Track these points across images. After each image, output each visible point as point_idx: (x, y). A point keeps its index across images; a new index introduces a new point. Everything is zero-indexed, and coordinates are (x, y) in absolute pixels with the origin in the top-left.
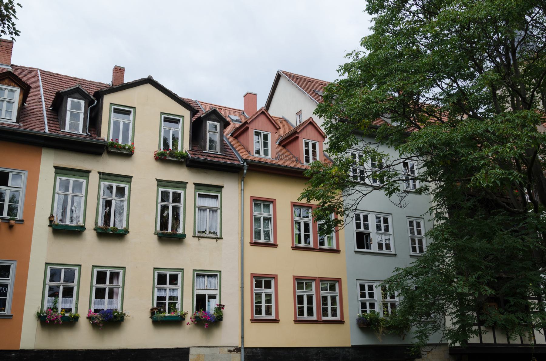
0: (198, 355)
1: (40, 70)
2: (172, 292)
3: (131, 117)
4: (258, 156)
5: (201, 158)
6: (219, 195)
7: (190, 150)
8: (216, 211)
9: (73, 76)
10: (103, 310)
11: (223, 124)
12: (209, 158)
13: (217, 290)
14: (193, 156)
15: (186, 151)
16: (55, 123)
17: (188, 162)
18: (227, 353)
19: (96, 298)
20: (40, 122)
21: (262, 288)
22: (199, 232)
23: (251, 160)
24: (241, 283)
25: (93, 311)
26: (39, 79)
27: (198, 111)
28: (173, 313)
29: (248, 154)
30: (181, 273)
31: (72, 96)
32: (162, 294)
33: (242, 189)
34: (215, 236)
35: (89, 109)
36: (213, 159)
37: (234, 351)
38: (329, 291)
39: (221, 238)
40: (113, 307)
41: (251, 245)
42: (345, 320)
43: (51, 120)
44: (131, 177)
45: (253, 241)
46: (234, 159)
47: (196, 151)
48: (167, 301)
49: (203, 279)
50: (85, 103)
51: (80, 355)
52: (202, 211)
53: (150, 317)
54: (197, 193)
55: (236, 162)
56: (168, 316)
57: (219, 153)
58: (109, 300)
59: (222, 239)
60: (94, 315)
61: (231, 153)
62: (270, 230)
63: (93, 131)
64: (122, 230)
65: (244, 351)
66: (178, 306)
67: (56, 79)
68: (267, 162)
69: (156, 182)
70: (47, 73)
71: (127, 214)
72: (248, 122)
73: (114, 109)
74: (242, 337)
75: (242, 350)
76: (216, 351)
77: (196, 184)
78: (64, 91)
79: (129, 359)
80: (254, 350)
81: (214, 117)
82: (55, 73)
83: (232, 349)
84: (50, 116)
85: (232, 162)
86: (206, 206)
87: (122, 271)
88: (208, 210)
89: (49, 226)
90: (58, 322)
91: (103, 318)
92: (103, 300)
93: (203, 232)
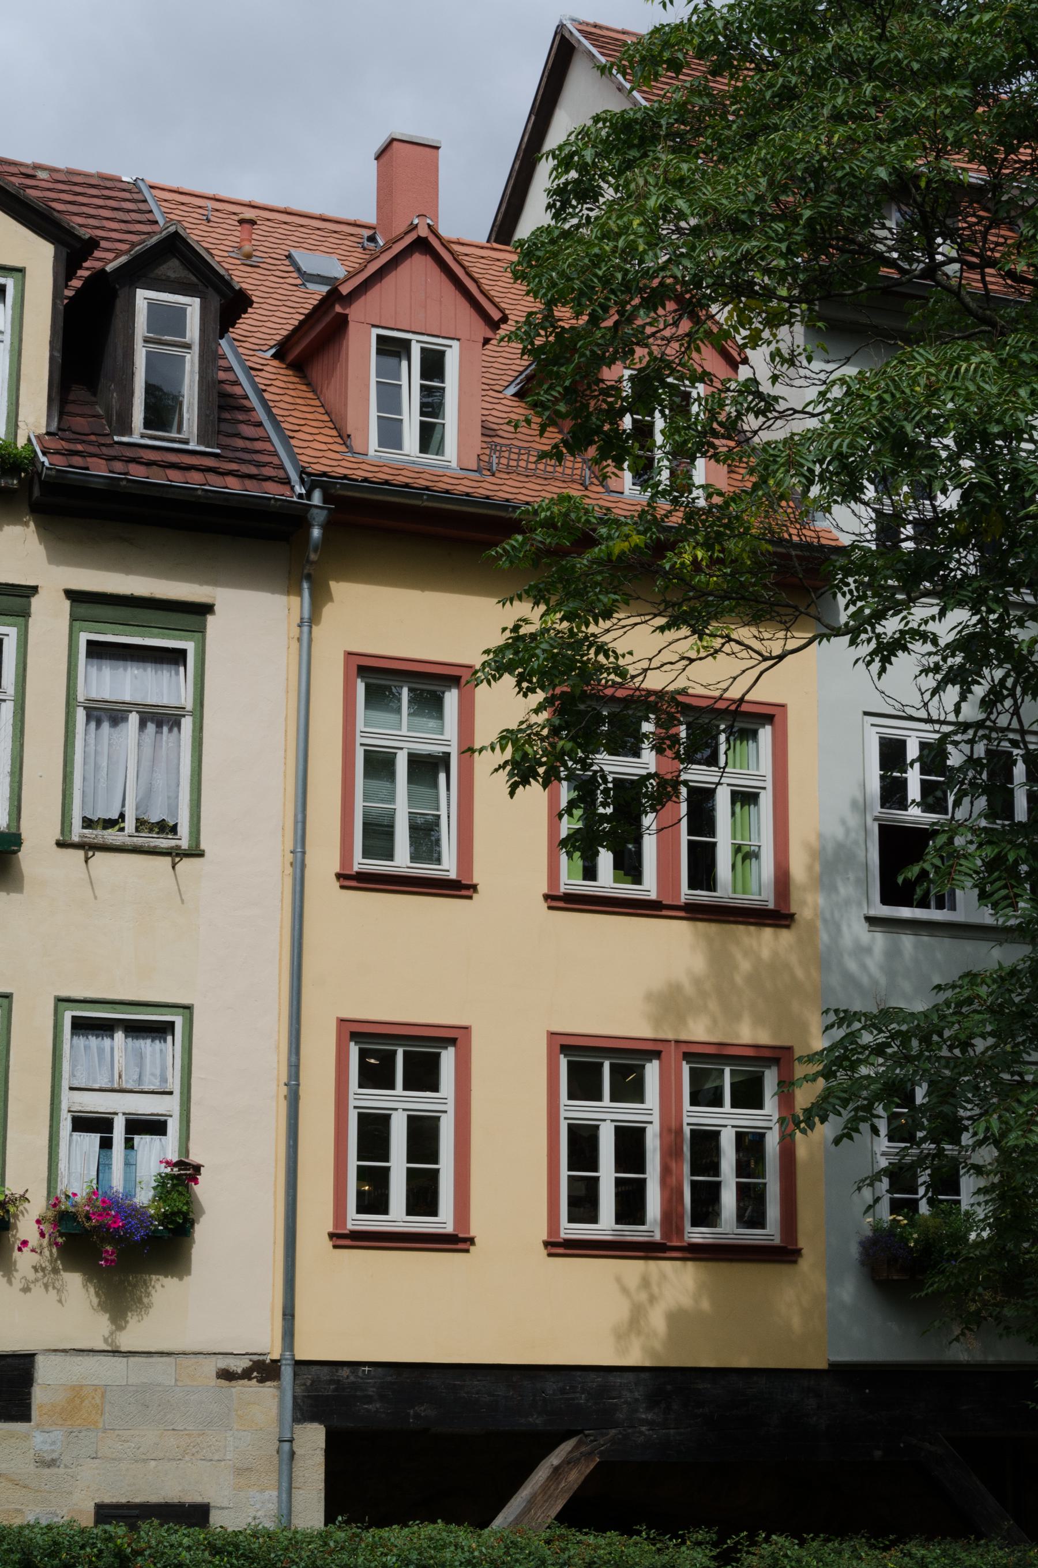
0: (73, 1388)
4: (390, 455)
5: (99, 469)
6: (189, 646)
7: (48, 433)
11: (216, 302)
12: (138, 473)
13: (171, 1093)
14: (60, 462)
15: (29, 440)
17: (36, 492)
18: (214, 1381)
21: (392, 1087)
23: (345, 477)
24: (290, 1066)
27: (93, 244)
29: (343, 448)
33: (302, 619)
34: (164, 843)
37: (246, 1374)
38: (727, 1107)
39: (196, 853)
41: (342, 887)
42: (802, 1243)
45: (356, 868)
46: (268, 471)
47: (79, 436)
49: (107, 1041)
52: (106, 726)
54: (84, 637)
55: (273, 490)
57: (192, 446)
59: (201, 854)
61: (259, 445)
62: (443, 813)
65: (296, 1375)
68: (427, 488)
72: (345, 290)
74: (289, 1314)
75: (287, 1372)
76: (160, 1371)
77: (74, 596)
80: (345, 1372)
81: (172, 268)
83: (239, 1365)
85: (254, 489)
86: (127, 698)
93: (109, 824)
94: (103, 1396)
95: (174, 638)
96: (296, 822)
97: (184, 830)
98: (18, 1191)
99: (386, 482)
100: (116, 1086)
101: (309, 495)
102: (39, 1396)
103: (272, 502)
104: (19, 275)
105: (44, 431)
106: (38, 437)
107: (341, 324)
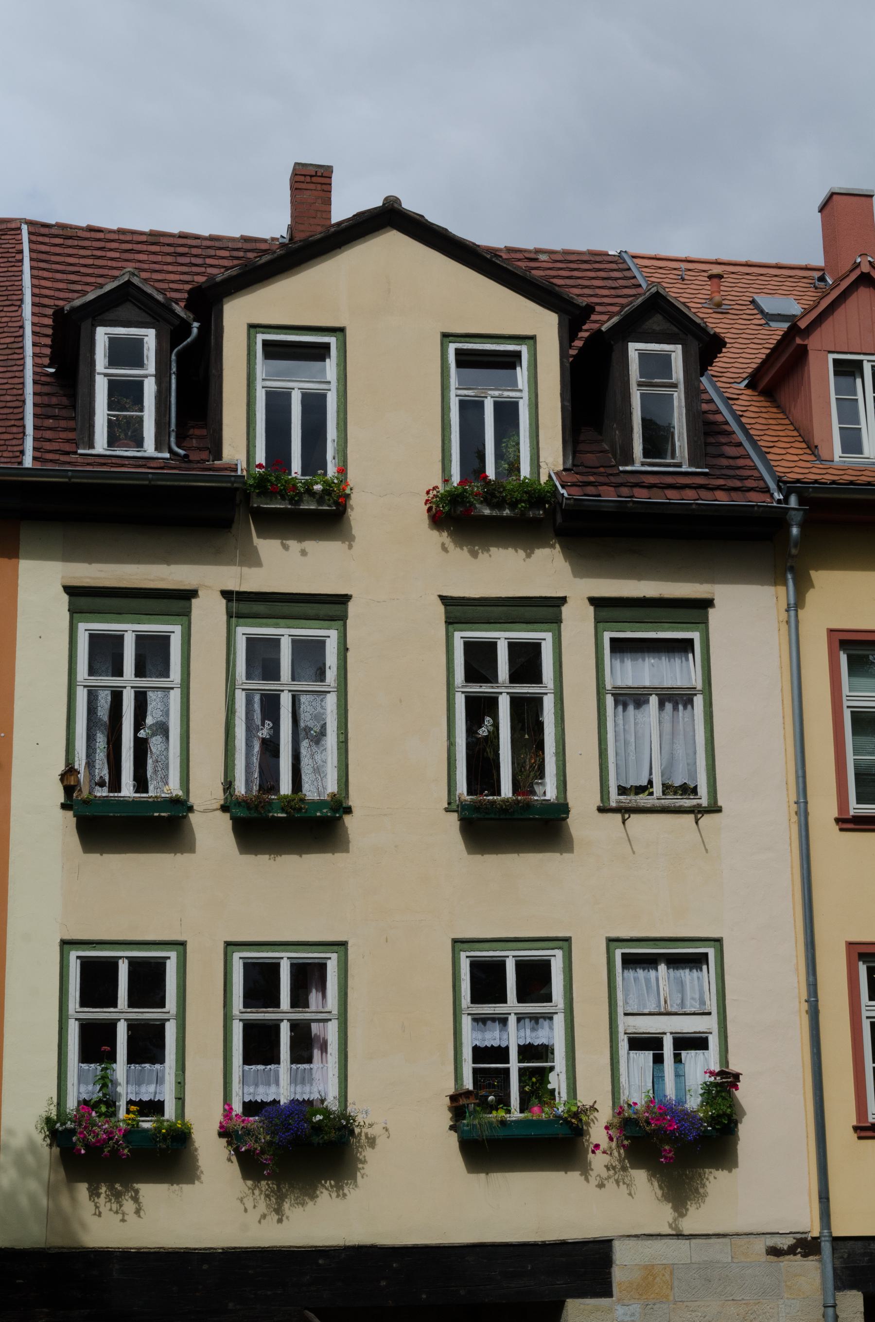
0: (646, 1267)
1: (30, 223)
2: (528, 1031)
3: (331, 367)
5: (609, 495)
6: (696, 636)
7: (565, 470)
8: (688, 701)
9: (146, 229)
10: (275, 1102)
11: (695, 346)
12: (641, 495)
13: (709, 1014)
14: (577, 492)
15: (550, 476)
16: (63, 424)
17: (559, 519)
18: (764, 1258)
19: (248, 1060)
20: (9, 429)
22: (622, 790)
24: (808, 985)
25: (238, 1108)
26: (21, 261)
27: (589, 310)
28: (536, 1109)
29: (812, 458)
30: (559, 953)
31: (110, 316)
32: (492, 1038)
33: (788, 605)
34: (687, 803)
35: (173, 357)
36: (658, 498)
37: (791, 1250)
40: (304, 1093)
41: (841, 830)
43: (49, 417)
44: (343, 600)
45: (852, 812)
46: (750, 483)
48: (514, 1065)
49: (652, 973)
50: (158, 337)
51: (205, 1267)
53: (452, 1128)
54: (607, 636)
55: (755, 499)
56: (518, 1122)
57: (684, 469)
58: (294, 1066)
59: (719, 810)
60: (237, 1125)
61: (741, 462)
63: (200, 438)
64: (321, 804)
65: (834, 1249)
66: (557, 1081)
67: (84, 248)
69: (441, 609)
70: (54, 231)
71: (339, 742)
73: (266, 343)
76: (719, 1251)
78: (77, 303)
79: (383, 1283)
81: (656, 322)
82: (83, 224)
83: (785, 1243)
84: (46, 400)
85: (739, 500)
86: (647, 683)
87: (334, 956)
88: (654, 700)
89: (64, 806)
90: (115, 1152)
91: (273, 1133)
92: (273, 1067)
93: (640, 790)
94: (672, 1273)
95: (683, 630)
96: (797, 778)
97: (703, 790)
98: (588, 1103)
99: (851, 483)
100: (663, 1010)
101: (786, 500)
102: (618, 1275)
103: (756, 508)
104: (531, 342)
105: (561, 468)
106: (557, 474)
107: (803, 352)
